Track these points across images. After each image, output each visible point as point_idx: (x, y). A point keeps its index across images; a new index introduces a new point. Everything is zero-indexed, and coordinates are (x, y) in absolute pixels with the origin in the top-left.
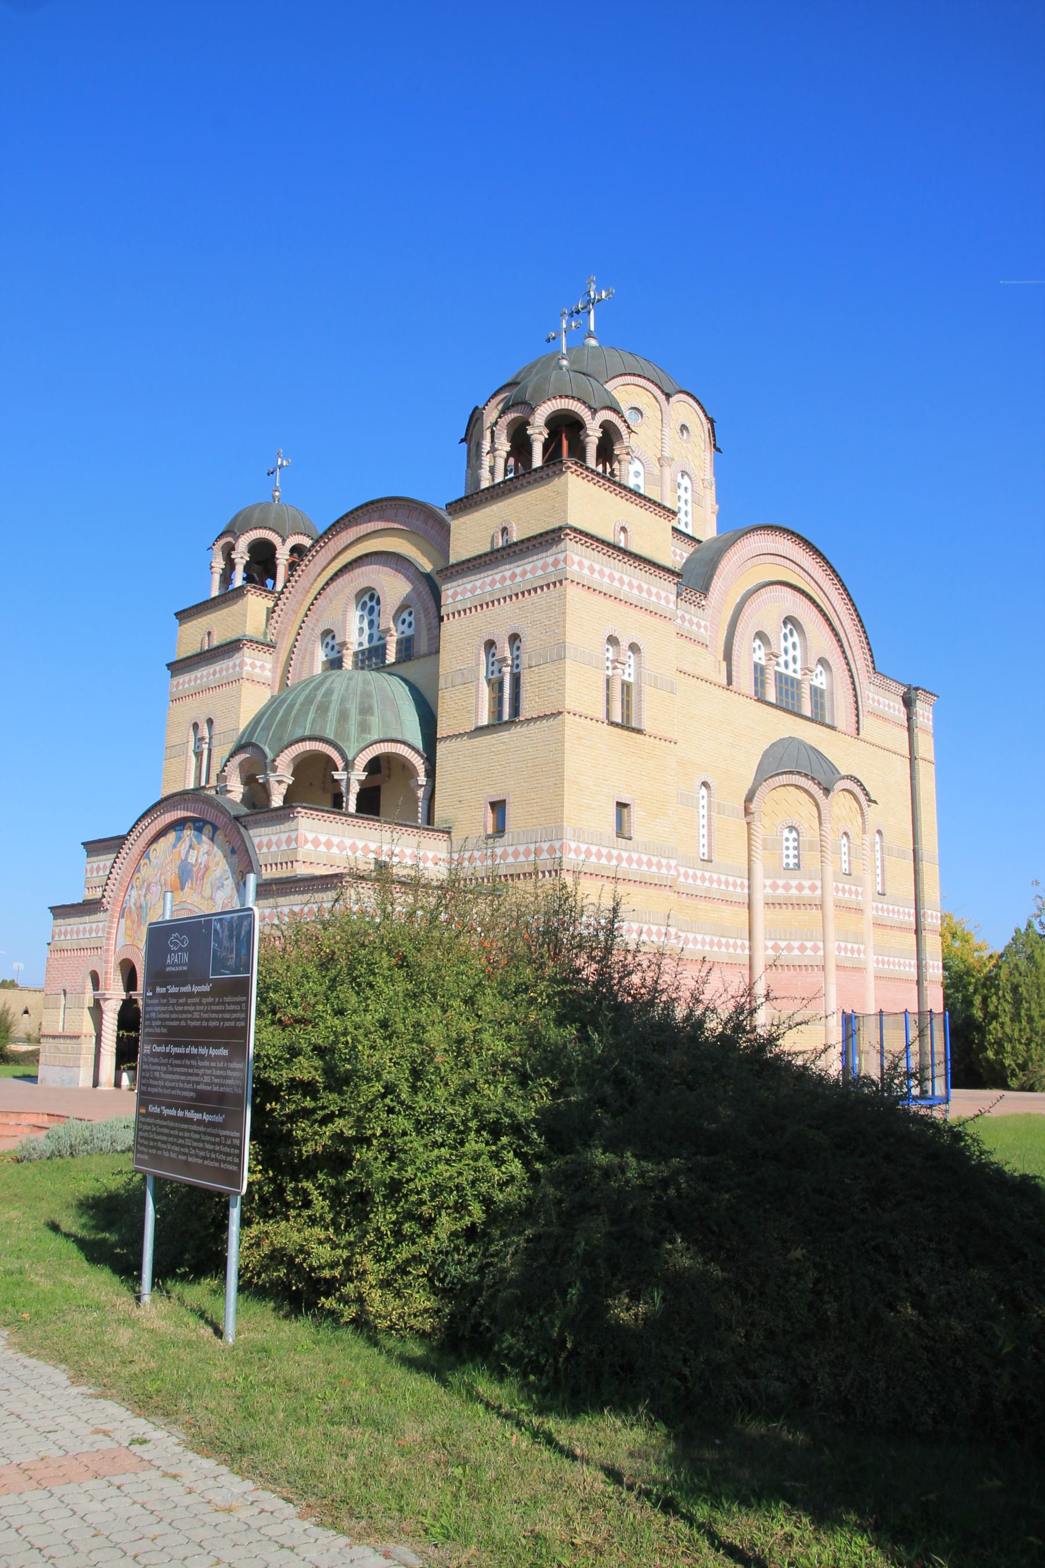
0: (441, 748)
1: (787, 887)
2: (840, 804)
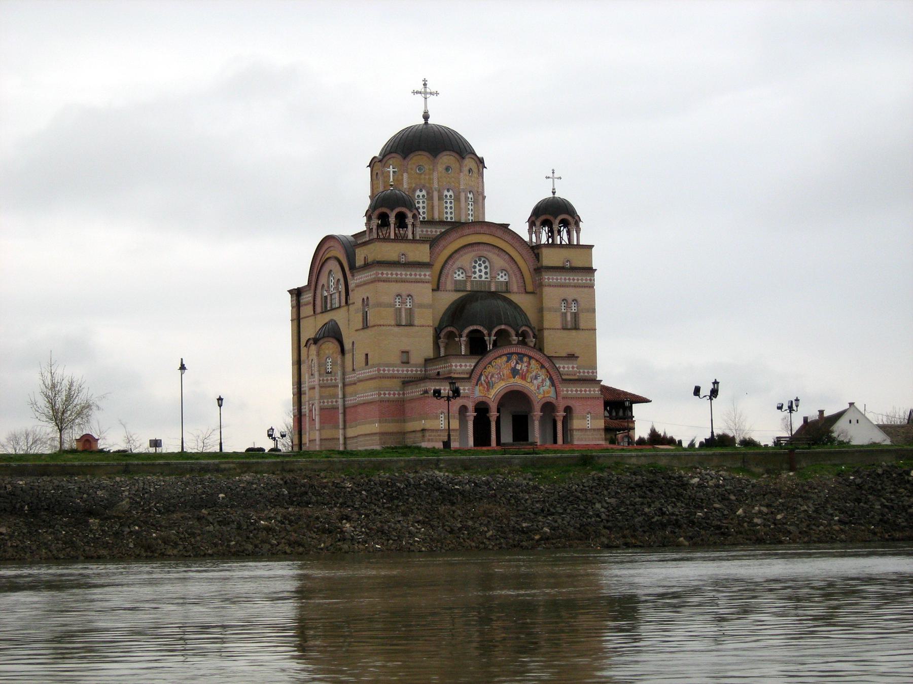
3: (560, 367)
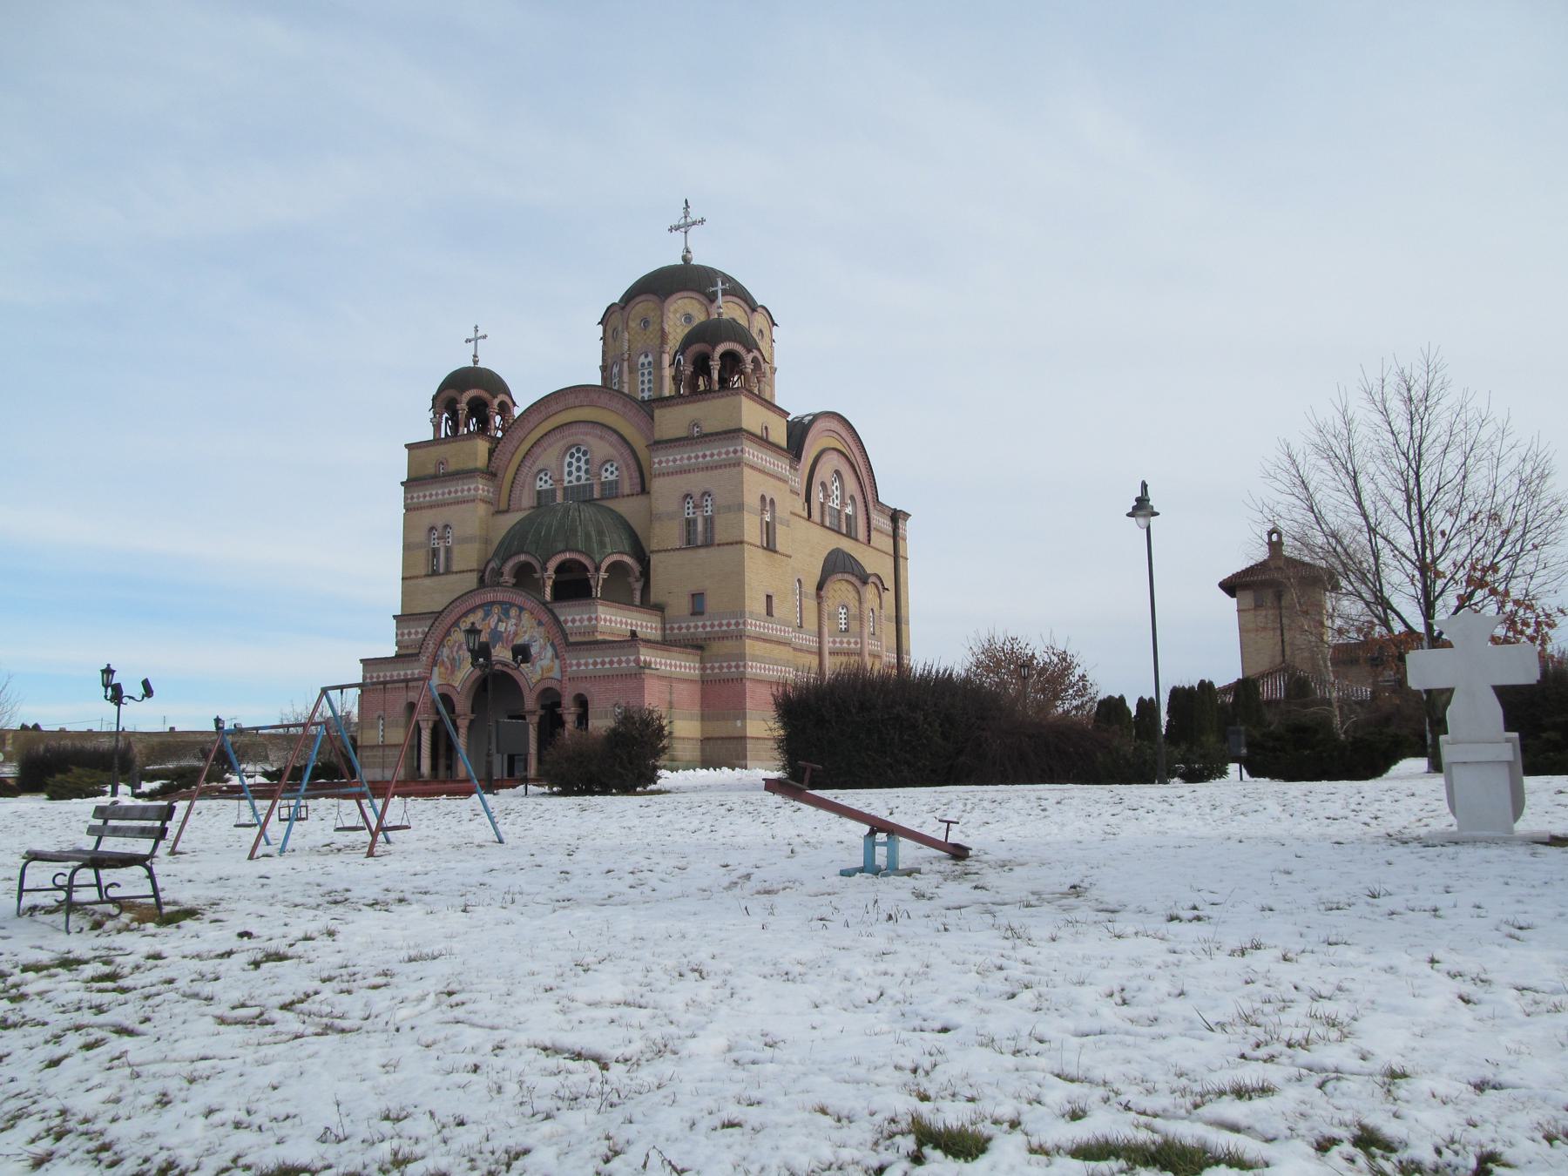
0: (654, 559)
1: (841, 642)
2: (870, 593)
3: (566, 622)
